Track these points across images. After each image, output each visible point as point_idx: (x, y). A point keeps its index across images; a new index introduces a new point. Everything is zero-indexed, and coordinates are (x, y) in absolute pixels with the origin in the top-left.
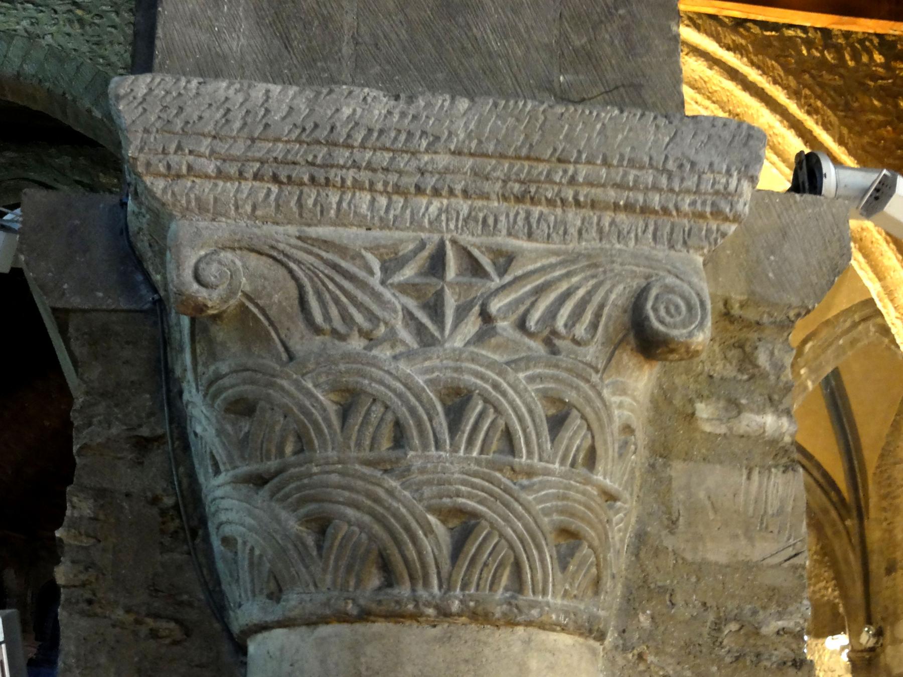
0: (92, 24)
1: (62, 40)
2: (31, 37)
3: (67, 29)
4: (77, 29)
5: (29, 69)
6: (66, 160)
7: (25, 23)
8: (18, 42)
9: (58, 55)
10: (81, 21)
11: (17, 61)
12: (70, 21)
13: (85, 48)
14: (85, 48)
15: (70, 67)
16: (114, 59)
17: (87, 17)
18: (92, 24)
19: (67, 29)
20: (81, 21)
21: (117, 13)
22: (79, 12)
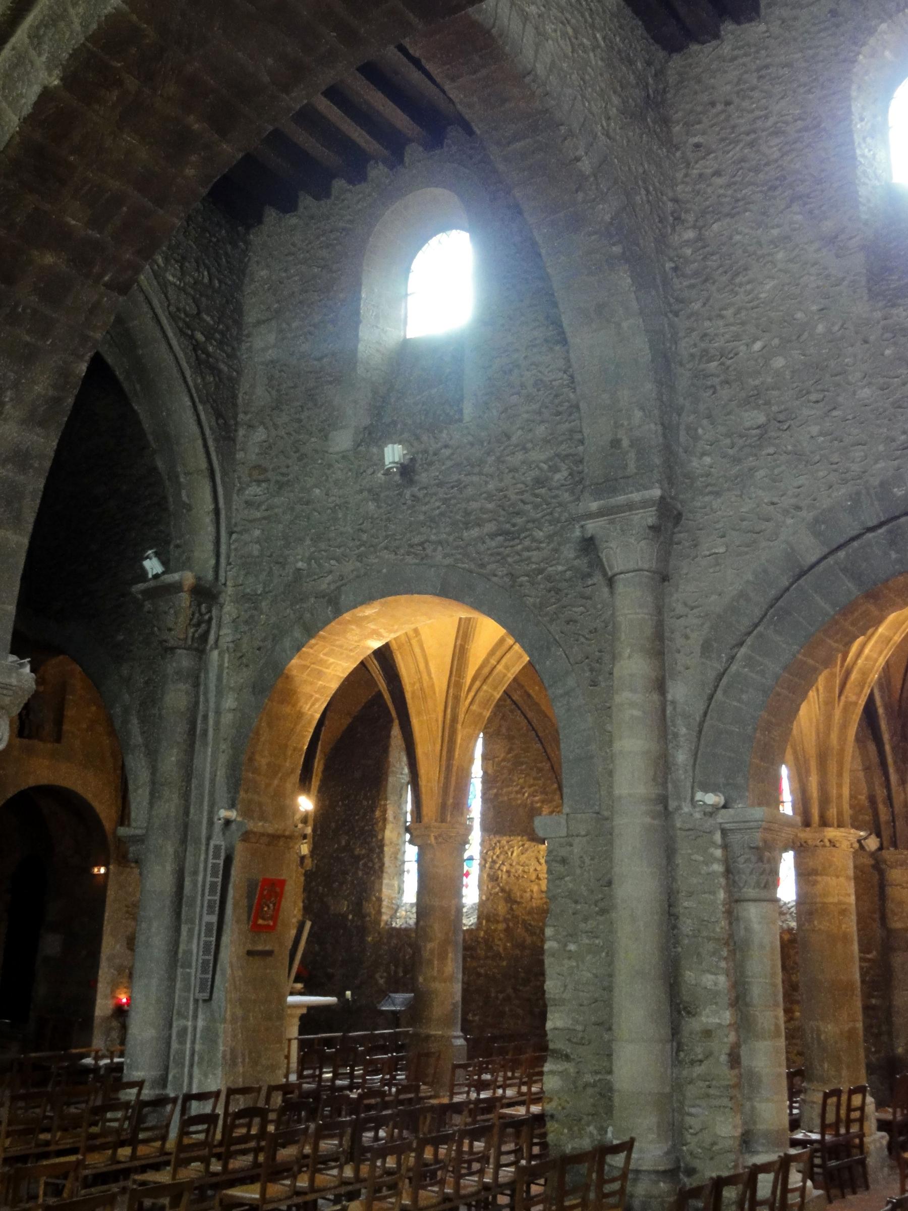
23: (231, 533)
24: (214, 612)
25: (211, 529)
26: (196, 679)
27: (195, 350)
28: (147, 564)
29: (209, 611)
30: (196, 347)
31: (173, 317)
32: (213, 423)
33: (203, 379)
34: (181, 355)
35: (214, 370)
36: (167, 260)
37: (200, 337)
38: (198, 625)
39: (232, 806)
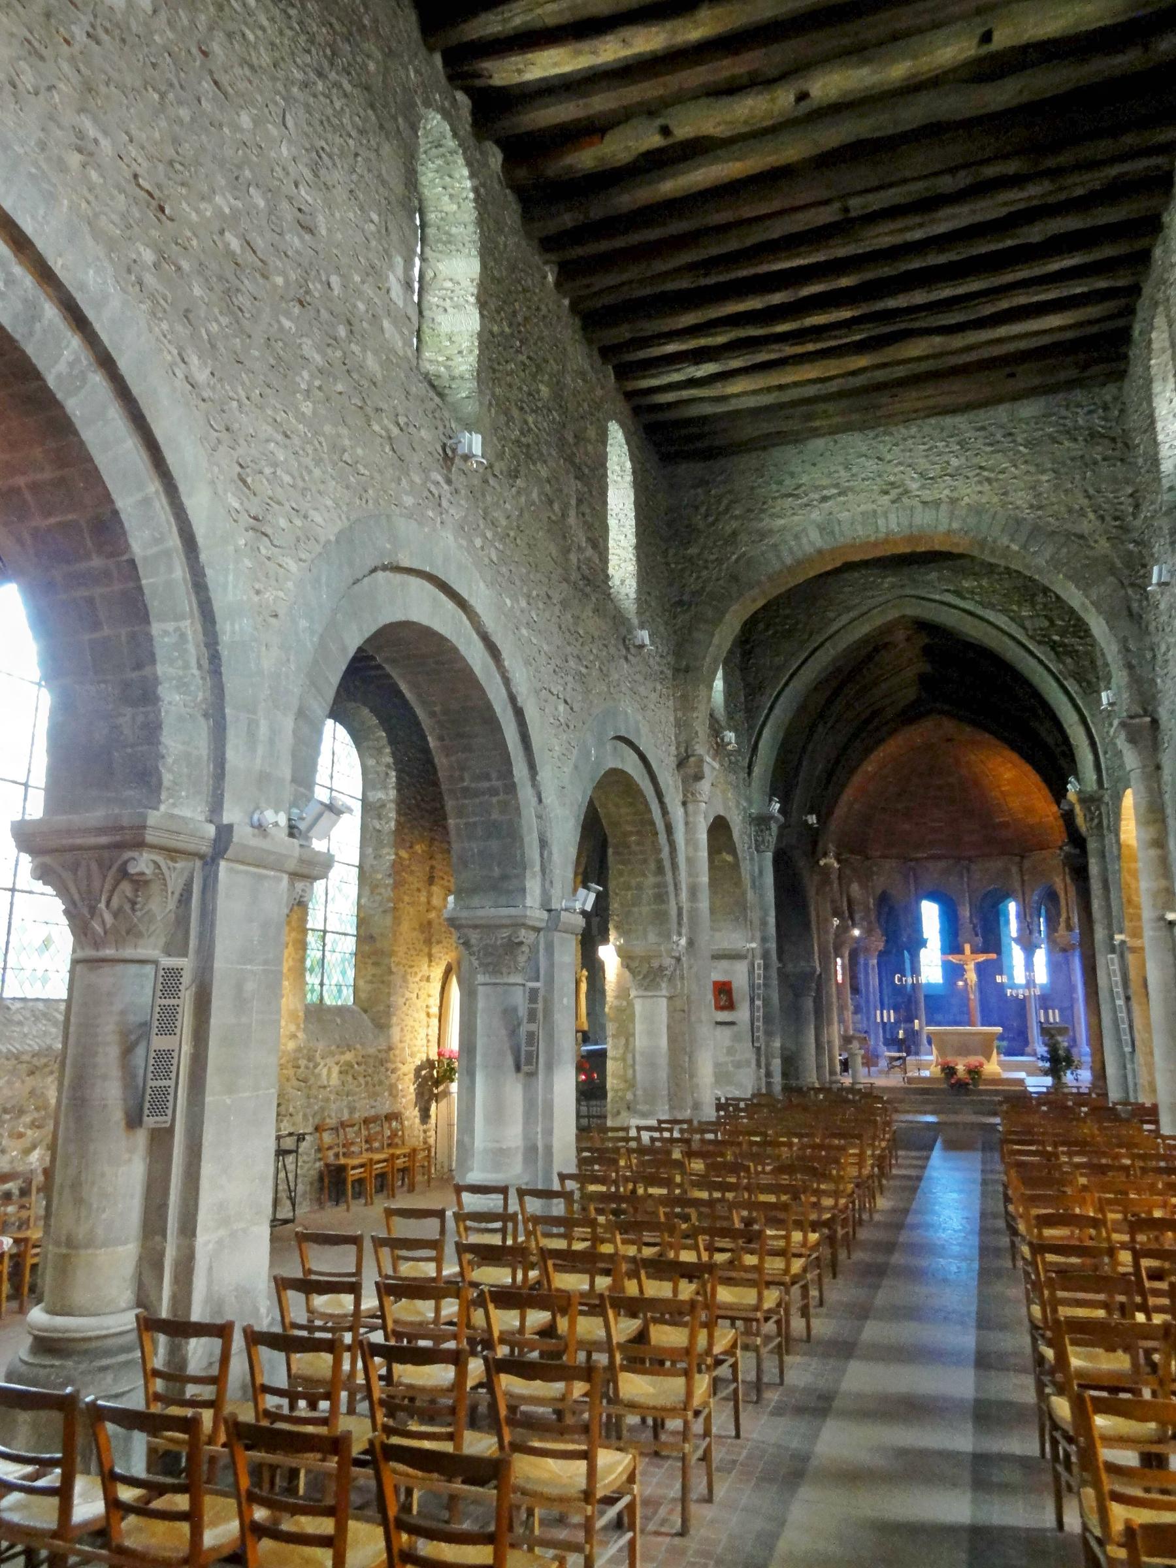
0: (997, 480)
1: (976, 497)
2: (953, 501)
3: (979, 488)
4: (986, 487)
5: (955, 525)
6: (934, 575)
7: (947, 492)
8: (944, 507)
9: (977, 510)
10: (988, 480)
11: (945, 521)
12: (980, 482)
13: (995, 500)
14: (995, 500)
15: (986, 518)
16: (1019, 502)
17: (992, 475)
18: (997, 480)
19: (979, 488)
20: (988, 480)
21: (1015, 466)
22: (986, 473)
23: (1105, 753)
24: (1103, 808)
25: (1090, 757)
26: (1103, 855)
27: (1053, 648)
28: (1069, 786)
29: (1098, 808)
30: (1054, 646)
31: (1031, 638)
32: (1077, 687)
33: (1064, 663)
34: (1043, 657)
35: (1073, 653)
36: (1019, 604)
37: (1056, 638)
38: (1092, 819)
39: (1121, 932)
